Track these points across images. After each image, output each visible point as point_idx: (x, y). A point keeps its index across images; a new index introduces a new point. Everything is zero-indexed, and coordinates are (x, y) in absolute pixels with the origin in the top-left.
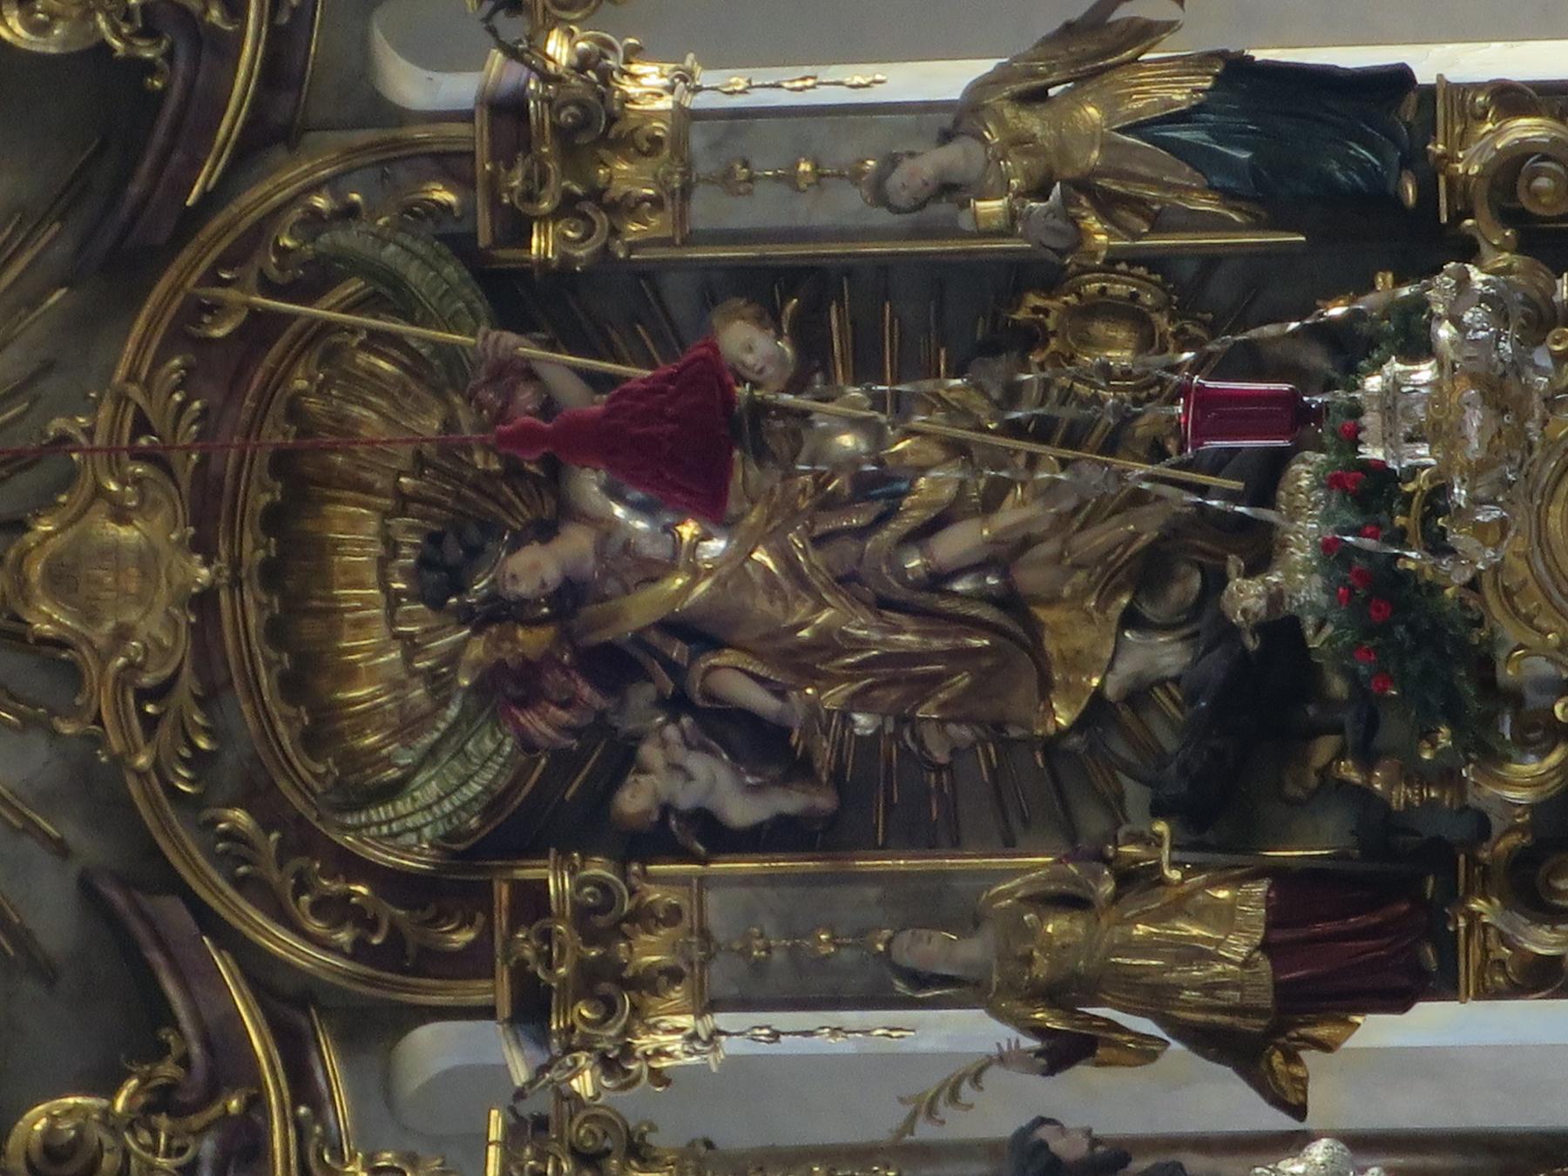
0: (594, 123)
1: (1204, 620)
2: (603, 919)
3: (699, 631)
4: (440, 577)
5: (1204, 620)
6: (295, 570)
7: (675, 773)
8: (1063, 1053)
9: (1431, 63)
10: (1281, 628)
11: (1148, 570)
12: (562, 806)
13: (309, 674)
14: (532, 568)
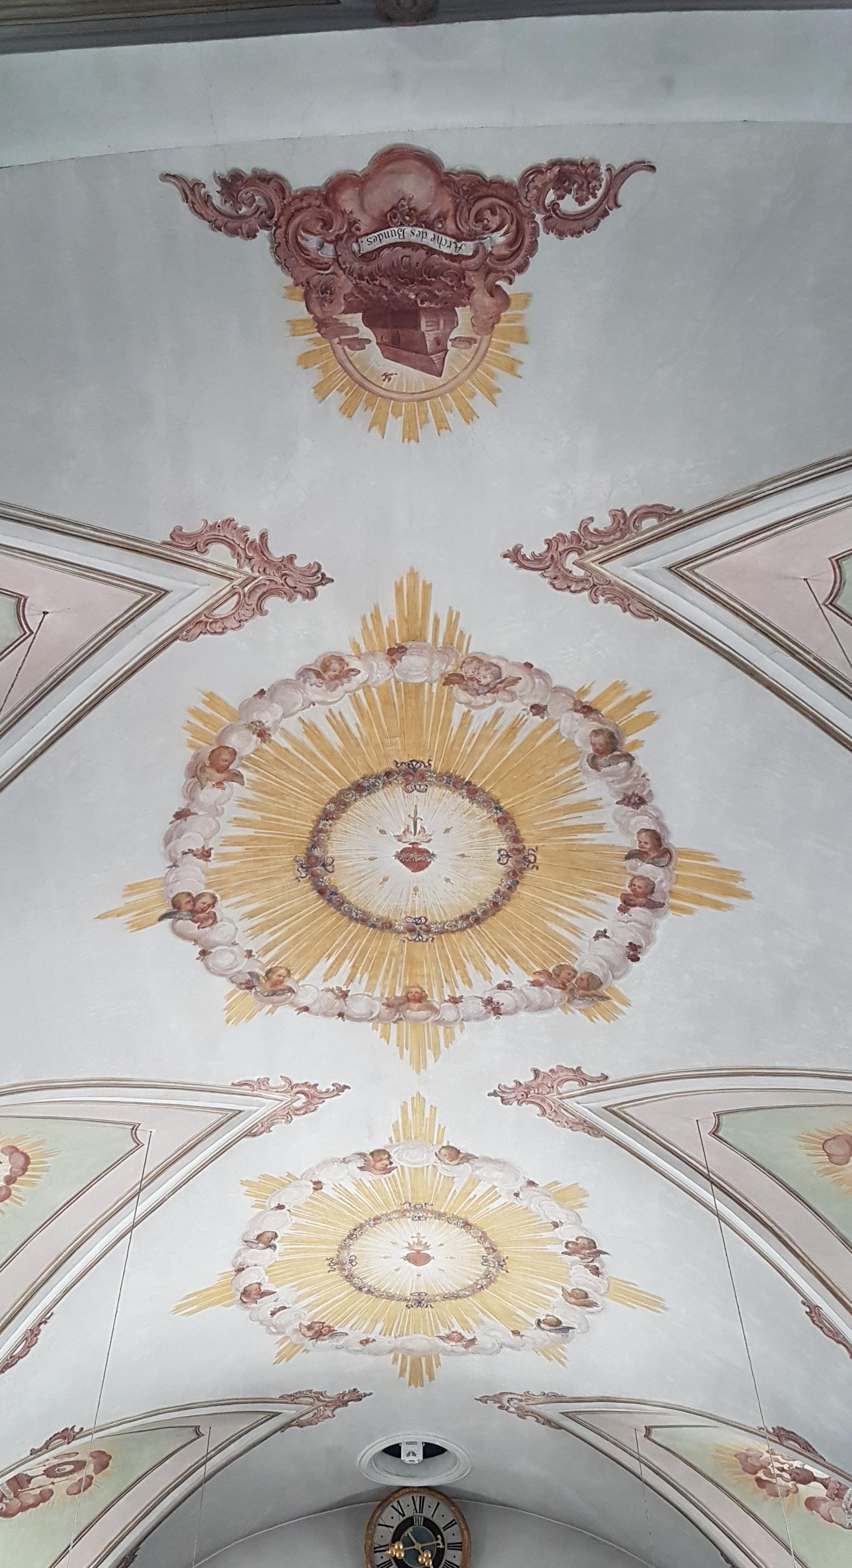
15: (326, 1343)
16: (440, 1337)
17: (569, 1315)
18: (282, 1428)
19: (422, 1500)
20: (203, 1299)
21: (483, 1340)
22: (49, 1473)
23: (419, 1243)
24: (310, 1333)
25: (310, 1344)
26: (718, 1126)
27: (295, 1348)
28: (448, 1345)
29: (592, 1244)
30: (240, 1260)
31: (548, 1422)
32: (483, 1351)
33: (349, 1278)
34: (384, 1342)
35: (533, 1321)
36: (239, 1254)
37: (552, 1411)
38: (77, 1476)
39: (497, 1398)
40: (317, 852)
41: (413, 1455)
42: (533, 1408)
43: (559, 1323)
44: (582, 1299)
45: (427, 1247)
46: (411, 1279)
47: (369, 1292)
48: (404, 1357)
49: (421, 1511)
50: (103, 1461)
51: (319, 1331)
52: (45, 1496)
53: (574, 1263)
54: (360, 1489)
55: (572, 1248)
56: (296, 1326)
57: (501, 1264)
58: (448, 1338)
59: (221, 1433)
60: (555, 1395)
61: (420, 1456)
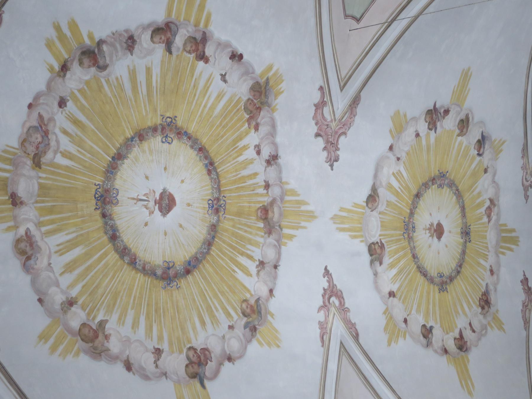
15: (492, 297)
16: (489, 221)
17: (474, 135)
20: (464, 376)
21: (491, 193)
23: (430, 229)
24: (486, 307)
25: (493, 309)
26: (354, 18)
27: (496, 319)
28: (494, 218)
29: (429, 113)
30: (439, 351)
32: (497, 194)
33: (451, 279)
34: (492, 259)
35: (478, 158)
36: (436, 351)
39: (526, 189)
40: (159, 272)
43: (479, 141)
44: (464, 124)
45: (432, 225)
46: (452, 237)
47: (460, 266)
48: (502, 247)
51: (485, 302)
53: (442, 126)
55: (432, 126)
56: (481, 317)
57: (442, 175)
58: (489, 216)
60: (523, 150)
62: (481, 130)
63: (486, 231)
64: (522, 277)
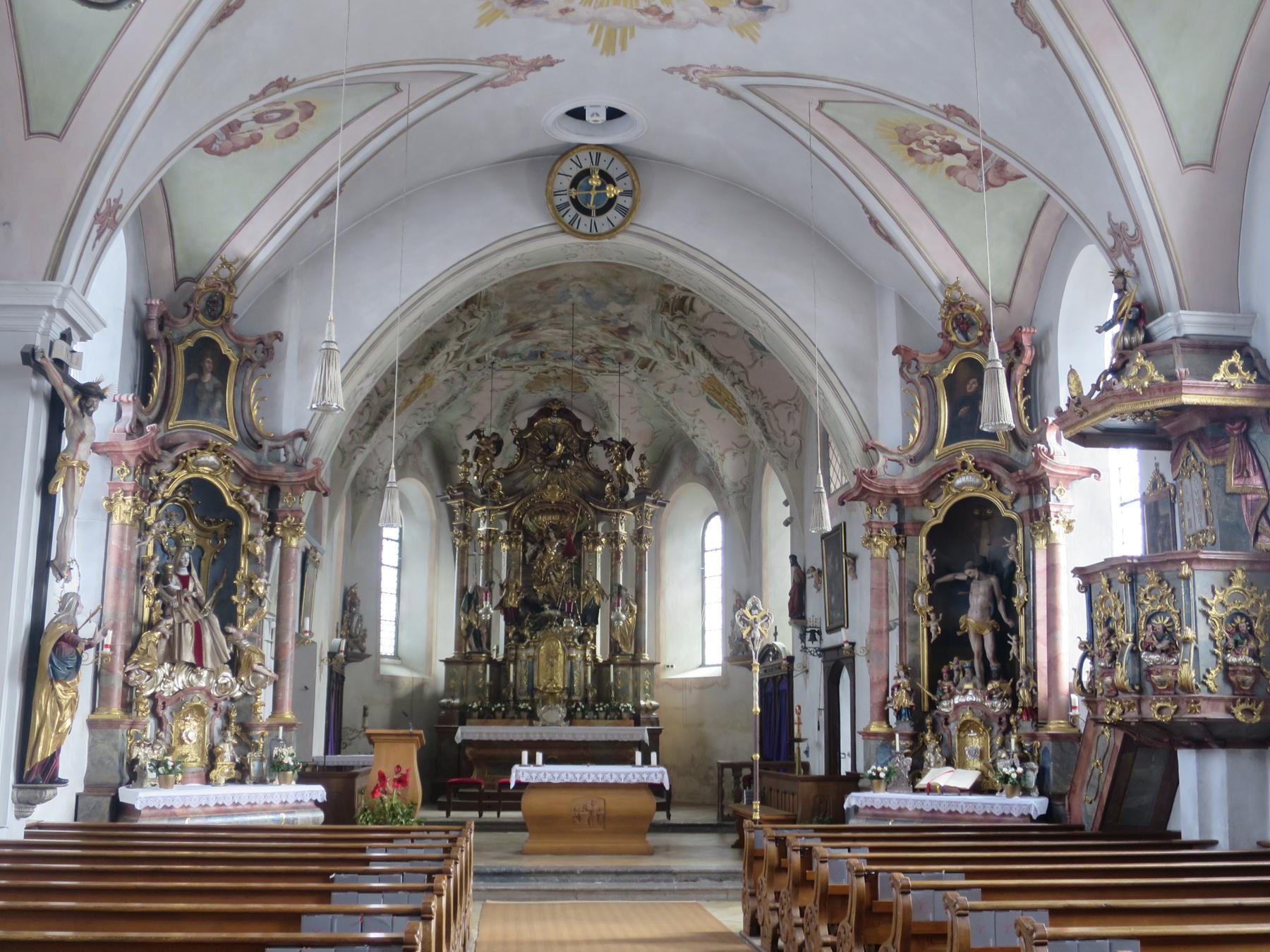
0: (596, 543)
1: (544, 602)
2: (517, 540)
3: (545, 551)
4: (552, 526)
5: (544, 602)
6: (552, 512)
7: (531, 548)
8: (501, 586)
9: (598, 627)
10: (543, 609)
11: (549, 596)
12: (528, 536)
13: (543, 512)
14: (552, 535)
16: (639, 10)
18: (477, 88)
19: (598, 155)
21: (681, 15)
22: (258, 119)
25: (510, 10)
28: (645, 18)
31: (728, 93)
37: (734, 83)
38: (286, 123)
39: (683, 70)
41: (596, 115)
42: (717, 80)
48: (600, 28)
49: (597, 163)
50: (308, 110)
52: (254, 140)
54: (542, 143)
58: (647, 11)
59: (419, 90)
60: (740, 69)
61: (603, 116)
62: (776, 5)
63: (625, 6)
64: (555, 58)
